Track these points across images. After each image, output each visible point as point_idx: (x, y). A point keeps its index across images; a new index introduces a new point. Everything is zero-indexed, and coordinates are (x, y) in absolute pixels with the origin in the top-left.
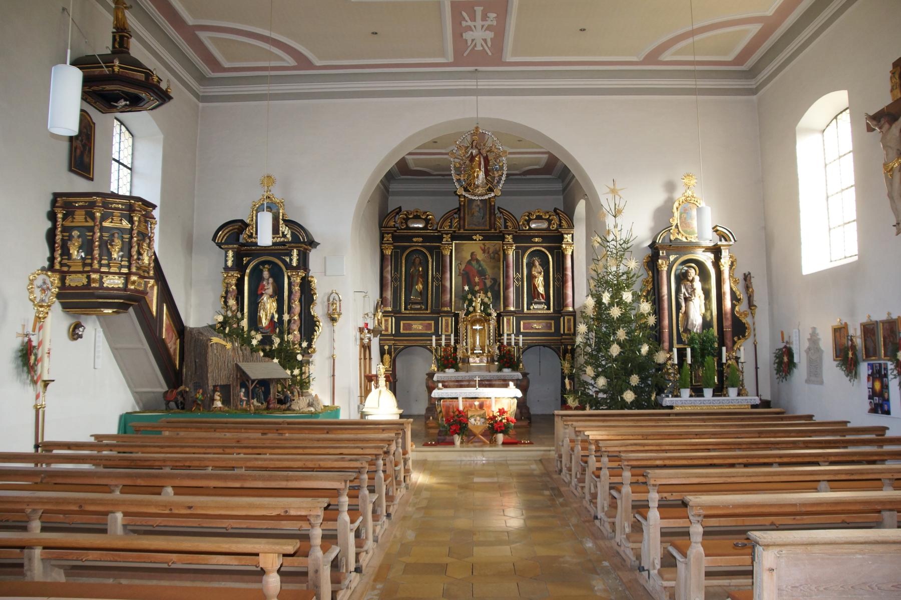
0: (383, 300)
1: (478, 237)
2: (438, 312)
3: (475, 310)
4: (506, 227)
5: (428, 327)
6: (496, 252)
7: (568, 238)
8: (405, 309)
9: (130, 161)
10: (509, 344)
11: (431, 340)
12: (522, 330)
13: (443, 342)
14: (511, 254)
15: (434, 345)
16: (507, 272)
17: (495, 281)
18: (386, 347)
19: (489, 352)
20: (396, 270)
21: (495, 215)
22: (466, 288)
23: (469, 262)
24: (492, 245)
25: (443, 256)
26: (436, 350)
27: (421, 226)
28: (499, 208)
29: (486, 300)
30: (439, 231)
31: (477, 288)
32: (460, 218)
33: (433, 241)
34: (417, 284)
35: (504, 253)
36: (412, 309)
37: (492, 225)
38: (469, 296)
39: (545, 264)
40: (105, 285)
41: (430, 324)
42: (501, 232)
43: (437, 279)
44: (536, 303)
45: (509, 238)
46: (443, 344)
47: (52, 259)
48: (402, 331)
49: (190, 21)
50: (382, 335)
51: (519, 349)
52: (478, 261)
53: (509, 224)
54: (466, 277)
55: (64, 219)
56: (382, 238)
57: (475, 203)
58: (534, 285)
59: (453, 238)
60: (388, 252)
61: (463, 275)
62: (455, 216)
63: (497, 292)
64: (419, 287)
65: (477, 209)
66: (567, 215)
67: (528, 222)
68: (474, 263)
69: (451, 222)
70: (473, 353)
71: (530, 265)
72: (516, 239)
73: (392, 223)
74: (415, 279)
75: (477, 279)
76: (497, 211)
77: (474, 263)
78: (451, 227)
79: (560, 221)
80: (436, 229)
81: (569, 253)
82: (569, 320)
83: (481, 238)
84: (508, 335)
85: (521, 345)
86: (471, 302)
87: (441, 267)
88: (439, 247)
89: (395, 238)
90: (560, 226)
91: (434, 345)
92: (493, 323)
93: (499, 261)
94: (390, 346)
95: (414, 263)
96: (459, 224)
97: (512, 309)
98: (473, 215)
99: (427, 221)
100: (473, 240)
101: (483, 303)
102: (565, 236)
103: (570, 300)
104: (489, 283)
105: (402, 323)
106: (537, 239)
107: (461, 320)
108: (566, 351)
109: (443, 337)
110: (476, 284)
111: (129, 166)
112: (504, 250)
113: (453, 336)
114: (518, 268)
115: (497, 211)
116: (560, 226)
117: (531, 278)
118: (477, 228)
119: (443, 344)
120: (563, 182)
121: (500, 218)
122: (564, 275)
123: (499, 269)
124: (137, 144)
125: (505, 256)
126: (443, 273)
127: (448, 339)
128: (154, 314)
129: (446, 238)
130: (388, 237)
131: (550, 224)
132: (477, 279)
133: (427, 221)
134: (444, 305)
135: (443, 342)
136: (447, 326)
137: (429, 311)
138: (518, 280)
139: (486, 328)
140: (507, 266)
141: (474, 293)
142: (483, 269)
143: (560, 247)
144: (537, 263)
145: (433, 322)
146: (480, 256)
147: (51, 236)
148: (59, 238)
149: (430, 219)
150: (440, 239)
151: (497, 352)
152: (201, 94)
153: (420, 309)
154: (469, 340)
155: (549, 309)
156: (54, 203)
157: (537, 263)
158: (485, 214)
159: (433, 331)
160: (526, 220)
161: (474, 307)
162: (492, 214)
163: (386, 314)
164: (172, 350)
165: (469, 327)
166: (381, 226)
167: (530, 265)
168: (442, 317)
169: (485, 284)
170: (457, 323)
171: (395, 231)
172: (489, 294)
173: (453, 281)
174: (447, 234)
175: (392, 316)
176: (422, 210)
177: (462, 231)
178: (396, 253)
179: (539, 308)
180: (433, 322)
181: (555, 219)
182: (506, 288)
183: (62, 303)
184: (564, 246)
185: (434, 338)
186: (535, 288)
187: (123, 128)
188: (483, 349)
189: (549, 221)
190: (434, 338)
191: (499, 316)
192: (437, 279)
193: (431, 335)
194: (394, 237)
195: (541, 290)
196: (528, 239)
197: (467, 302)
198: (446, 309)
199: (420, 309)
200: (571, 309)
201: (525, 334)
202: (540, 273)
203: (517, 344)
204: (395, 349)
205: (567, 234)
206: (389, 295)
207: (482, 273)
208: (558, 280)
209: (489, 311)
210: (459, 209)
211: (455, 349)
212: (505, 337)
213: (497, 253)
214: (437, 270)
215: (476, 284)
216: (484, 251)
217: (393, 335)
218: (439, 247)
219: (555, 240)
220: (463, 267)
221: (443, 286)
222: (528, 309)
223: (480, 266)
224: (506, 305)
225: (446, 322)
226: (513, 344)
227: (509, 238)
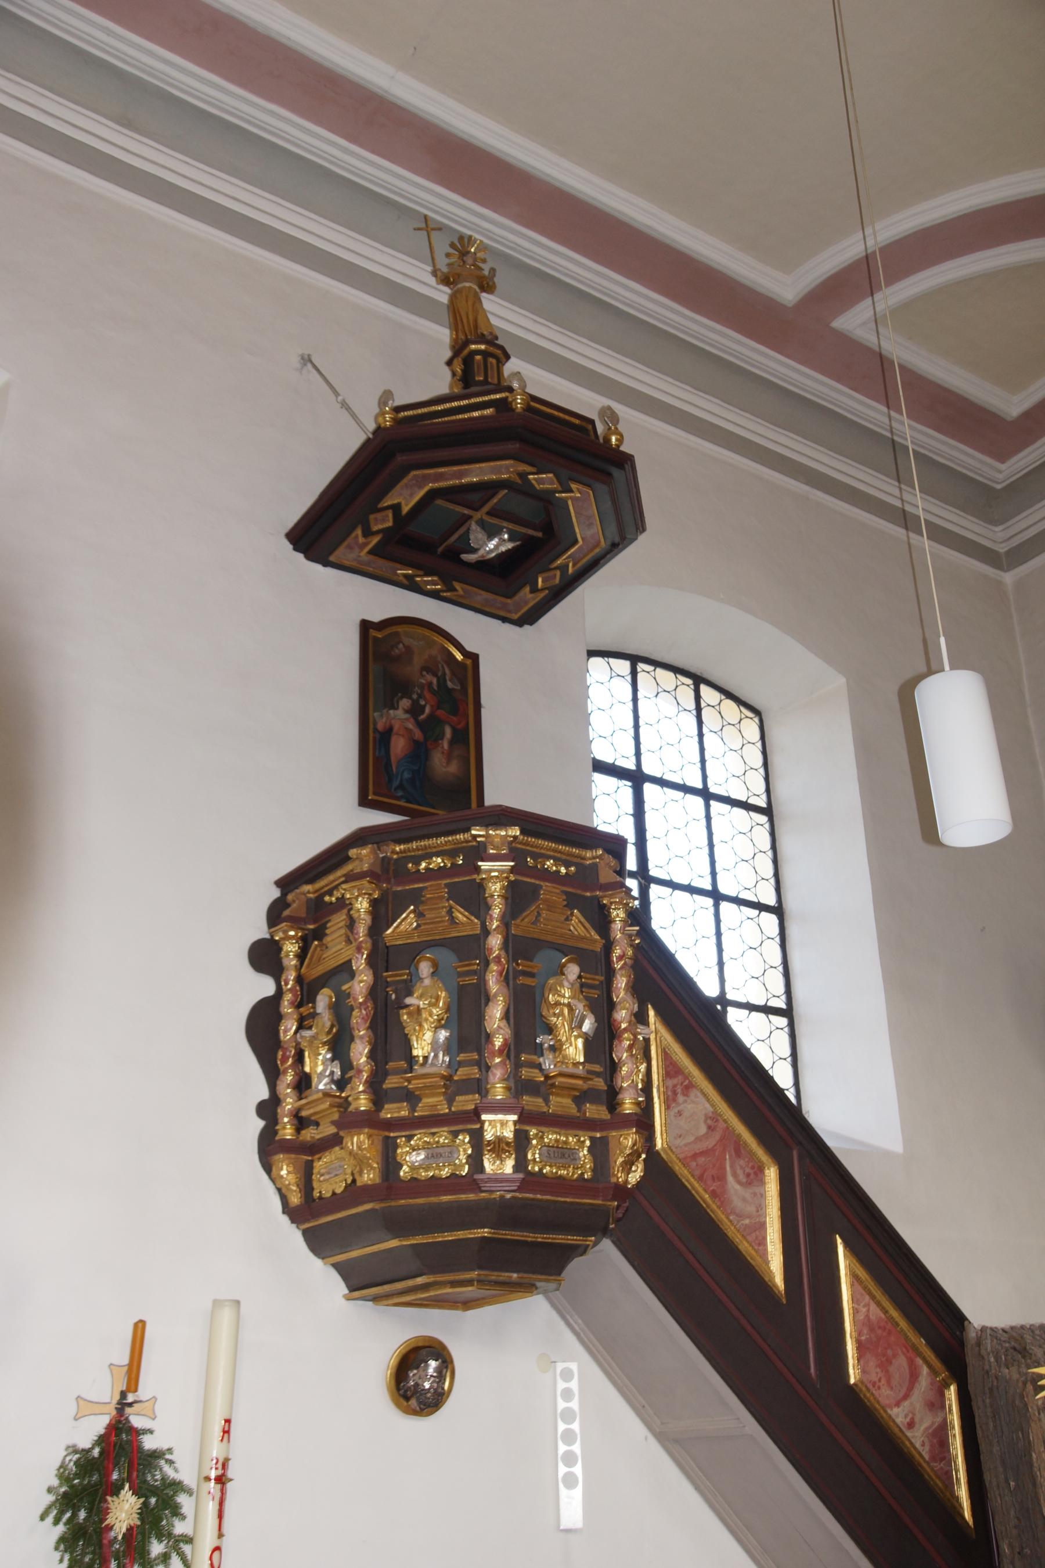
9: (760, 787)
40: (404, 1172)
47: (268, 1109)
49: (786, 287)
55: (301, 956)
111: (762, 803)
124: (777, 735)
128: (779, 1280)
147: (262, 1027)
148: (288, 1029)
152: (1002, 549)
156: (275, 914)
164: (918, 1440)
183: (344, 1270)
187: (708, 695)
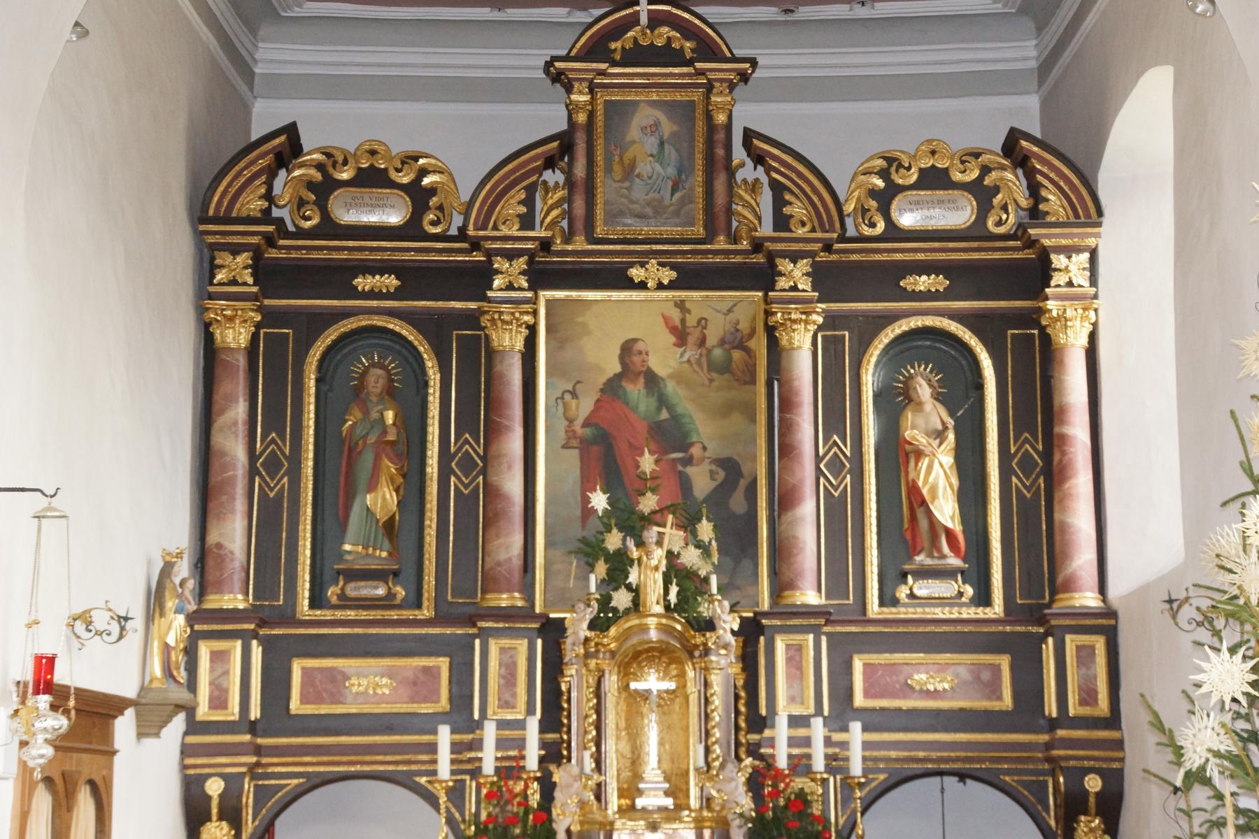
0: (205, 558)
1: (655, 272)
2: (466, 616)
3: (637, 605)
4: (782, 222)
5: (422, 685)
6: (736, 340)
7: (1070, 269)
8: (317, 601)
10: (800, 765)
11: (432, 748)
12: (859, 700)
13: (489, 760)
14: (802, 344)
15: (444, 769)
16: (788, 427)
17: (731, 469)
18: (214, 787)
19: (708, 802)
20: (274, 420)
21: (731, 172)
22: (599, 501)
23: (612, 388)
24: (721, 309)
25: (491, 353)
26: (457, 793)
27: (394, 218)
28: (749, 135)
29: (691, 557)
30: (475, 245)
31: (648, 503)
32: (570, 183)
33: (449, 280)
34: (372, 487)
35: (773, 342)
36: (346, 602)
37: (717, 219)
38: (613, 541)
39: (961, 393)
41: (432, 673)
42: (757, 246)
43: (467, 465)
44: (924, 573)
45: (796, 275)
46: (489, 767)
48: (295, 706)
50: (194, 726)
51: (848, 785)
52: (652, 380)
53: (797, 209)
54: (602, 454)
56: (207, 269)
58: (914, 490)
59: (541, 277)
60: (235, 336)
61: (585, 446)
62: (553, 177)
63: (740, 521)
64: (383, 499)
65: (651, 144)
66: (1056, 164)
67: (885, 198)
68: (635, 390)
69: (529, 202)
70: (629, 811)
71: (894, 401)
72: (830, 280)
73: (253, 204)
74: (367, 459)
75: (647, 463)
76: (739, 154)
77: (635, 390)
78: (527, 221)
79: (1034, 190)
80: (462, 235)
81: (1074, 341)
82: (1085, 654)
83: (667, 275)
84: (795, 721)
85: (856, 768)
86: (619, 566)
87: (478, 408)
88: (472, 320)
89: (271, 276)
90: (1035, 214)
91: (444, 769)
92: (724, 665)
93: (753, 381)
94: (232, 782)
95: (358, 392)
96: (569, 214)
97: (810, 596)
98: (629, 171)
99: (419, 196)
100: (630, 285)
101: (675, 571)
102: (1059, 260)
103: (1083, 560)
104: (702, 481)
105: (297, 667)
106: (923, 282)
107: (572, 649)
108: (1073, 805)
109: (490, 733)
110: (645, 484)
112: (771, 331)
113: (533, 724)
114: (837, 410)
115: (739, 154)
116: (1035, 214)
117: (896, 455)
118: (647, 229)
119: (489, 767)
120: (1040, 29)
121: (754, 187)
122: (1052, 442)
123: (753, 419)
125: (776, 351)
126: (494, 431)
127: (511, 742)
129: (508, 275)
130: (236, 268)
131: (984, 208)
132: (647, 463)
133: (419, 196)
134: (491, 583)
135: (489, 760)
136: (509, 679)
137: (427, 612)
138: (836, 466)
139: (693, 690)
140: (788, 404)
141: (634, 525)
142: (675, 418)
143: (1032, 318)
144: (924, 391)
145: (443, 663)
146: (663, 358)
149: (432, 191)
150: (476, 280)
151: (745, 802)
153: (387, 602)
154: (611, 747)
155: (984, 598)
157: (924, 391)
158: (683, 170)
159: (444, 704)
160: (873, 193)
161: (636, 591)
162: (717, 163)
163: (206, 624)
165: (611, 682)
166: (200, 215)
167: (894, 401)
168: (484, 634)
169: (685, 485)
170: (554, 666)
171: (270, 241)
172: (706, 530)
173: (539, 472)
174: (510, 255)
175: (246, 637)
176: (399, 146)
177: (580, 244)
178: (276, 343)
179: (937, 596)
180: (443, 663)
181: (1013, 184)
182: (784, 501)
184: (1051, 304)
185: (444, 736)
186: (918, 501)
188: (677, 789)
189: (983, 193)
190: (444, 736)
191: (751, 631)
192: (467, 465)
193: (428, 724)
194: (261, 269)
195: (946, 510)
196: (886, 279)
197: (601, 568)
198: (504, 600)
199: (387, 602)
200: (1088, 599)
201: (874, 721)
202: (940, 435)
203: (836, 763)
204: (262, 795)
205: (1069, 251)
206: (234, 534)
207: (671, 436)
208: (1027, 464)
209: (705, 610)
210: (565, 142)
211: (548, 789)
212: (781, 731)
213: (741, 346)
214: (467, 422)
215: (645, 484)
216: (680, 335)
217: (253, 728)
218: (472, 320)
219: (1011, 285)
220: (584, 407)
221: (493, 493)
222: (887, 599)
223: (663, 401)
224: (781, 585)
225: (507, 659)
226: (819, 764)
227: (796, 275)
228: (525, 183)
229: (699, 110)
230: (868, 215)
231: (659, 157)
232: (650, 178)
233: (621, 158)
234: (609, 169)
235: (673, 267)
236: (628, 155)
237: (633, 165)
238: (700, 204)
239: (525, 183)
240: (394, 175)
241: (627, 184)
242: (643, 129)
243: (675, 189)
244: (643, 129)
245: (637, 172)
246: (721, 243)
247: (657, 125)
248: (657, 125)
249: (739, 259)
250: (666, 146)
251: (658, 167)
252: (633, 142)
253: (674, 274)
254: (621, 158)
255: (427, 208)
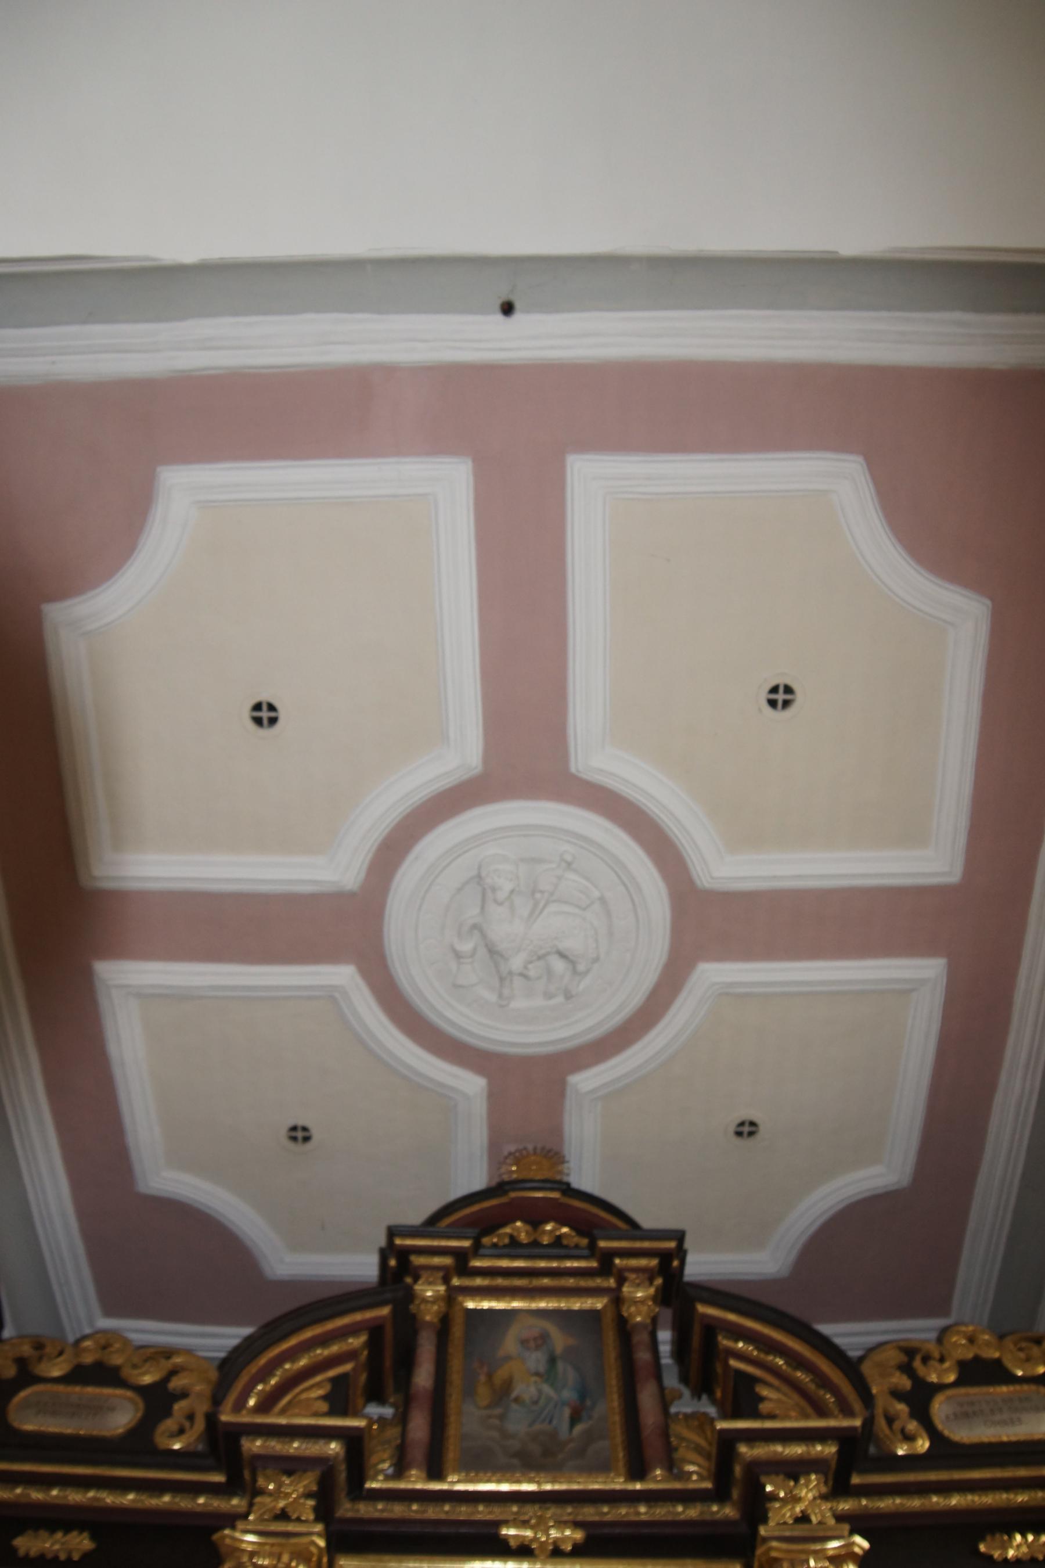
57: (510, 1344)
65: (536, 1360)
98: (503, 1393)
228: (332, 1373)
229: (608, 1320)
230: (897, 1425)
231: (549, 1374)
232: (536, 1403)
233: (490, 1376)
234: (469, 1391)
235: (577, 1525)
236: (501, 1374)
237: (508, 1385)
238: (618, 1435)
239: (332, 1373)
240: (127, 1373)
241: (498, 1411)
242: (524, 1342)
243: (575, 1419)
244: (524, 1342)
245: (514, 1395)
246: (658, 1480)
247: (543, 1339)
248: (543, 1339)
249: (693, 1512)
250: (560, 1365)
251: (546, 1389)
252: (508, 1358)
253: (579, 1535)
254: (490, 1376)
255: (168, 1413)
